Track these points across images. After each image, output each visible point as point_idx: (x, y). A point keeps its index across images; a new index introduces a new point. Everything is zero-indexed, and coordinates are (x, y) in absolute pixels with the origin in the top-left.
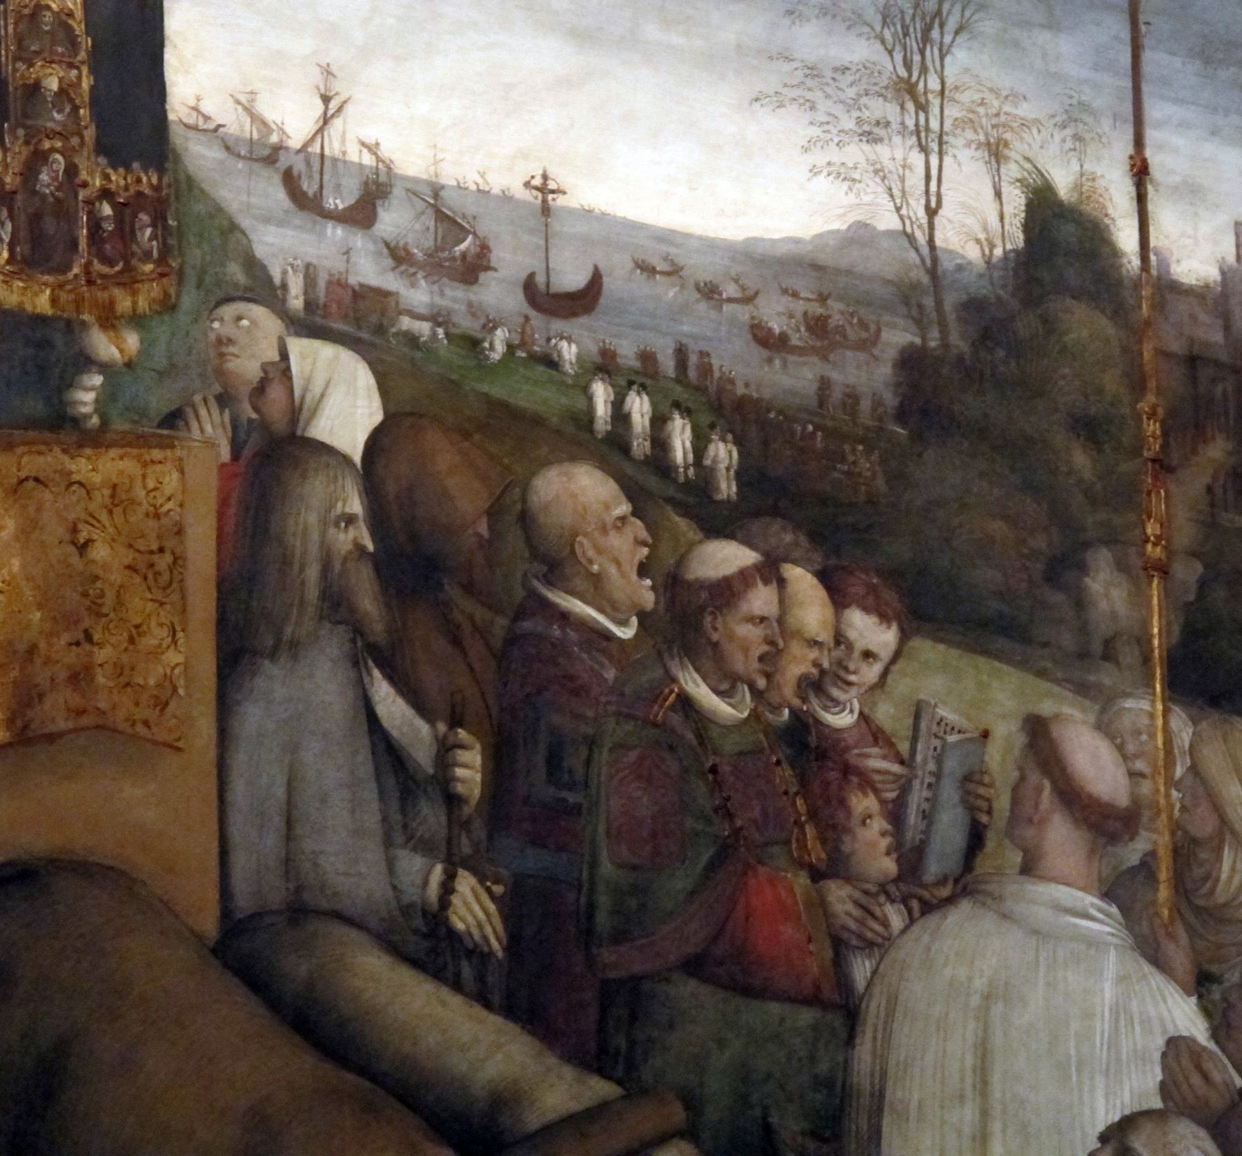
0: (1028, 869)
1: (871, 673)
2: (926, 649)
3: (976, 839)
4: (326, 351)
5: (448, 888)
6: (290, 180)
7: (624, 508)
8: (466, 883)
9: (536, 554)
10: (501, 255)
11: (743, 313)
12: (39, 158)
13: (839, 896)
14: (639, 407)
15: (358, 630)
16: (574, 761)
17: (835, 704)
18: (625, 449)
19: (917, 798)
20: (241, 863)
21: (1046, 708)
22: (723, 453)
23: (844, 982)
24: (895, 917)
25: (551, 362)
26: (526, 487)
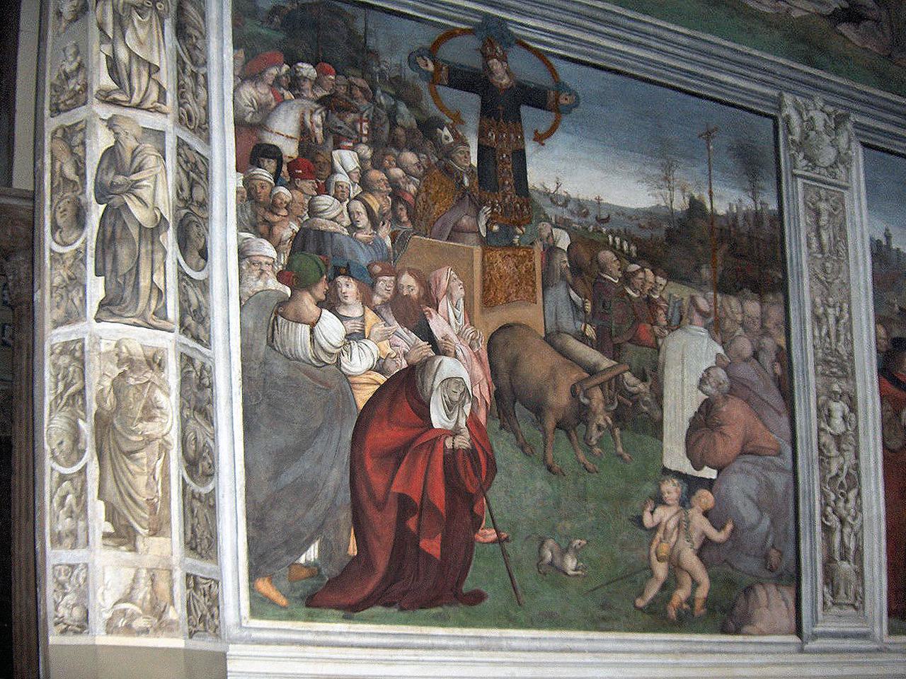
0: (691, 324)
1: (662, 288)
2: (671, 283)
3: (681, 319)
4: (560, 231)
5: (585, 327)
6: (551, 199)
7: (615, 259)
8: (588, 326)
9: (599, 267)
10: (590, 212)
11: (635, 222)
12: (504, 197)
13: (656, 329)
14: (617, 240)
15: (568, 282)
16: (607, 305)
17: (654, 294)
18: (615, 248)
19: (670, 310)
20: (547, 324)
21: (694, 294)
22: (633, 248)
23: (657, 345)
24: (666, 331)
25: (601, 232)
26: (597, 254)
